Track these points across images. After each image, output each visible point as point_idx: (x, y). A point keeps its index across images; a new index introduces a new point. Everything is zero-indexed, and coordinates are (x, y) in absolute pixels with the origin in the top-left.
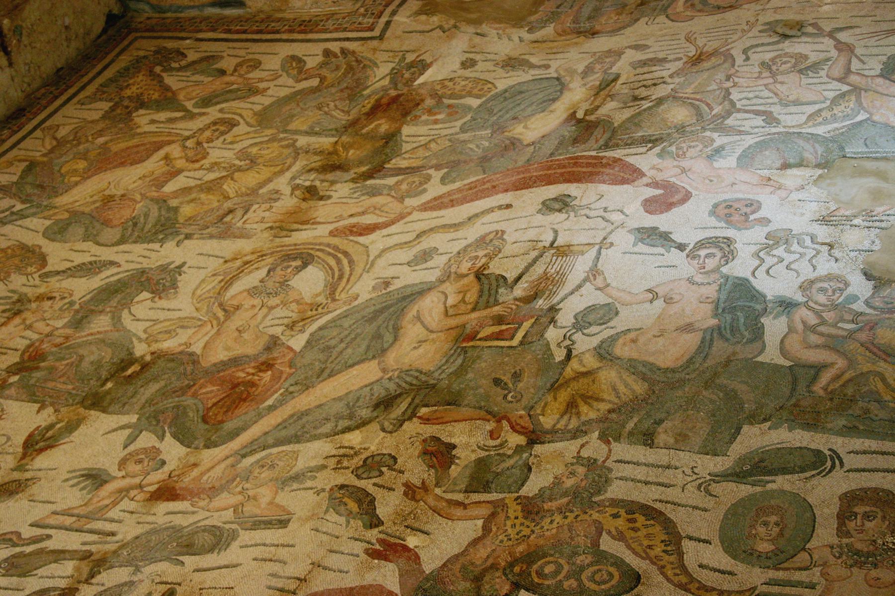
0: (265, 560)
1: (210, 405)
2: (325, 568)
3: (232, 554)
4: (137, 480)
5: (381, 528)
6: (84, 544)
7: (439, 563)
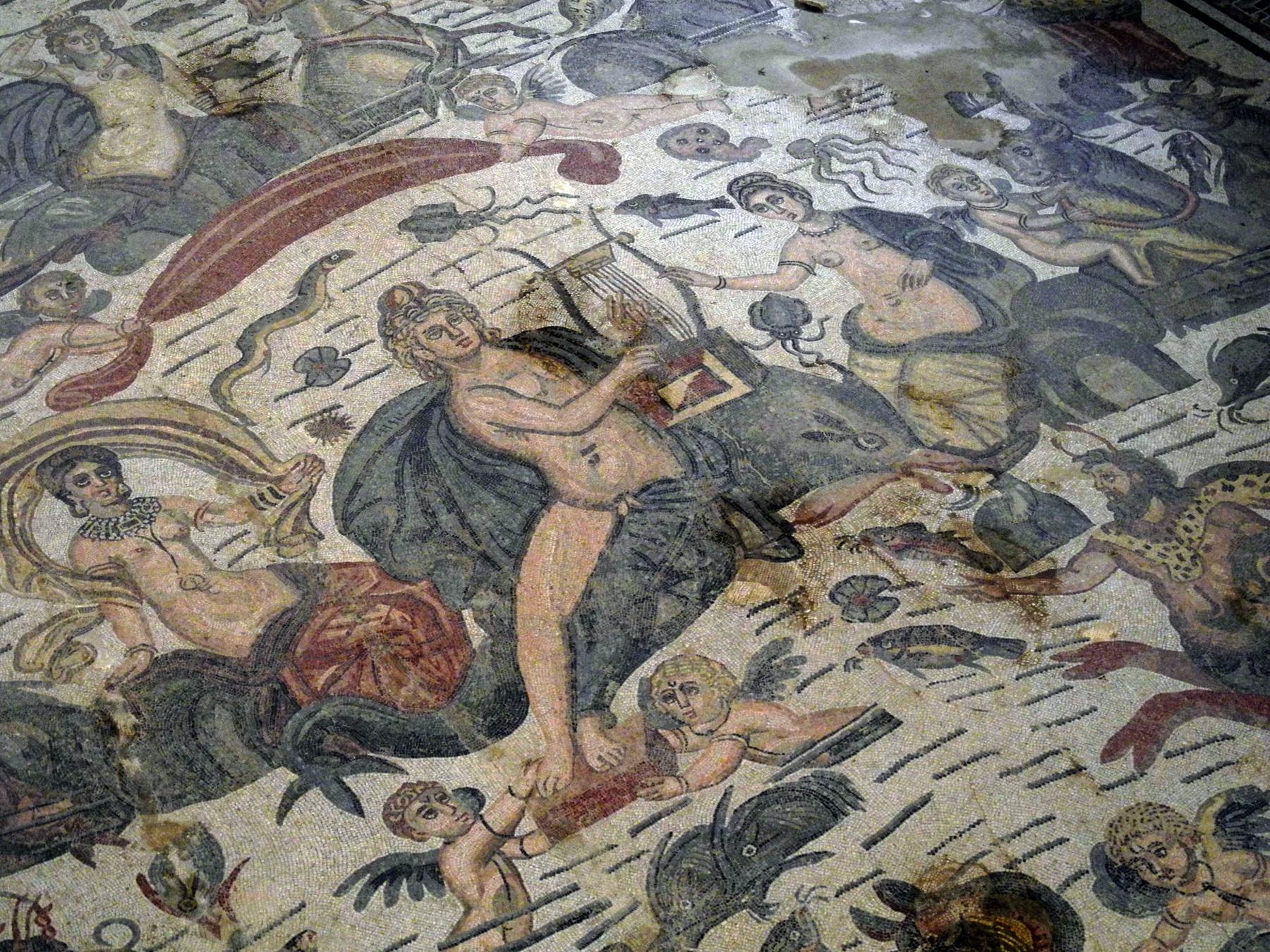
4: (479, 834)
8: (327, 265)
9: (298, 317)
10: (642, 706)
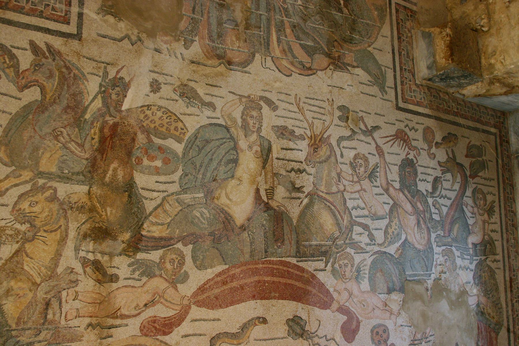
8: (257, 323)
9: (235, 342)
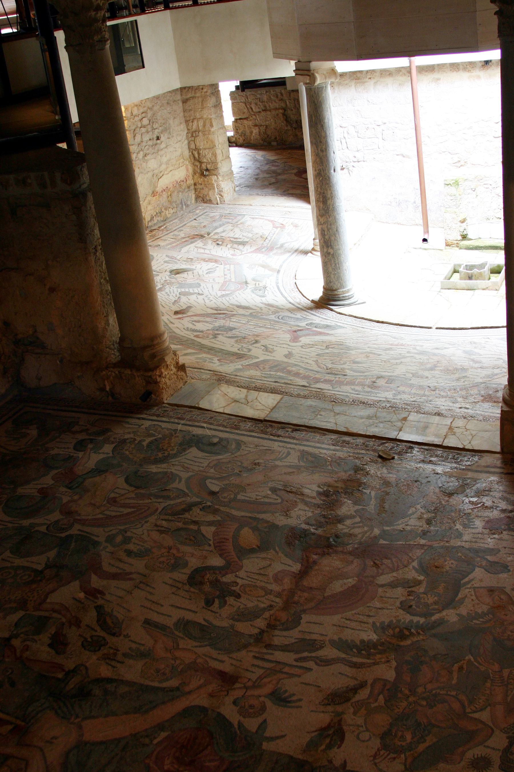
0: (156, 603)
1: (209, 747)
2: (126, 590)
3: (177, 615)
4: (249, 693)
5: (96, 605)
6: (272, 654)
7: (72, 584)
10: (172, 678)
